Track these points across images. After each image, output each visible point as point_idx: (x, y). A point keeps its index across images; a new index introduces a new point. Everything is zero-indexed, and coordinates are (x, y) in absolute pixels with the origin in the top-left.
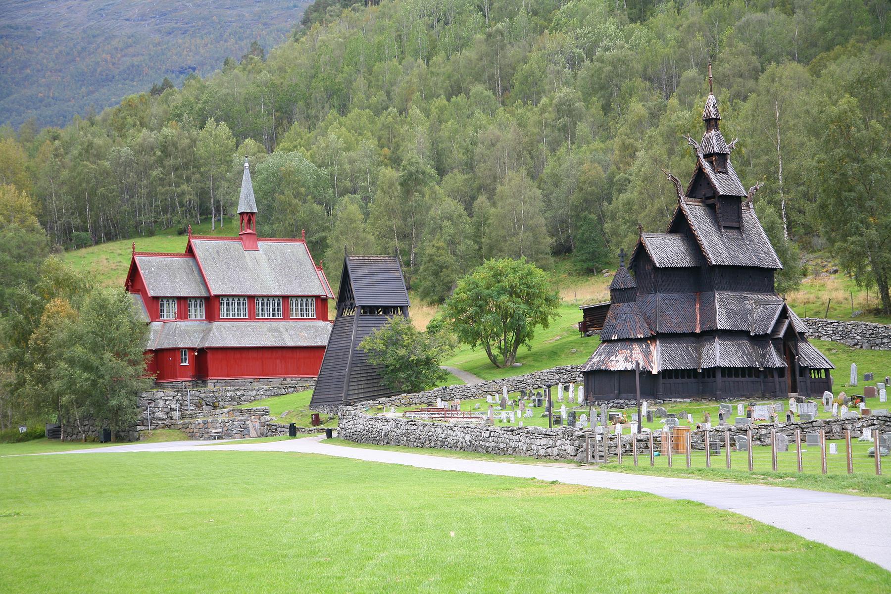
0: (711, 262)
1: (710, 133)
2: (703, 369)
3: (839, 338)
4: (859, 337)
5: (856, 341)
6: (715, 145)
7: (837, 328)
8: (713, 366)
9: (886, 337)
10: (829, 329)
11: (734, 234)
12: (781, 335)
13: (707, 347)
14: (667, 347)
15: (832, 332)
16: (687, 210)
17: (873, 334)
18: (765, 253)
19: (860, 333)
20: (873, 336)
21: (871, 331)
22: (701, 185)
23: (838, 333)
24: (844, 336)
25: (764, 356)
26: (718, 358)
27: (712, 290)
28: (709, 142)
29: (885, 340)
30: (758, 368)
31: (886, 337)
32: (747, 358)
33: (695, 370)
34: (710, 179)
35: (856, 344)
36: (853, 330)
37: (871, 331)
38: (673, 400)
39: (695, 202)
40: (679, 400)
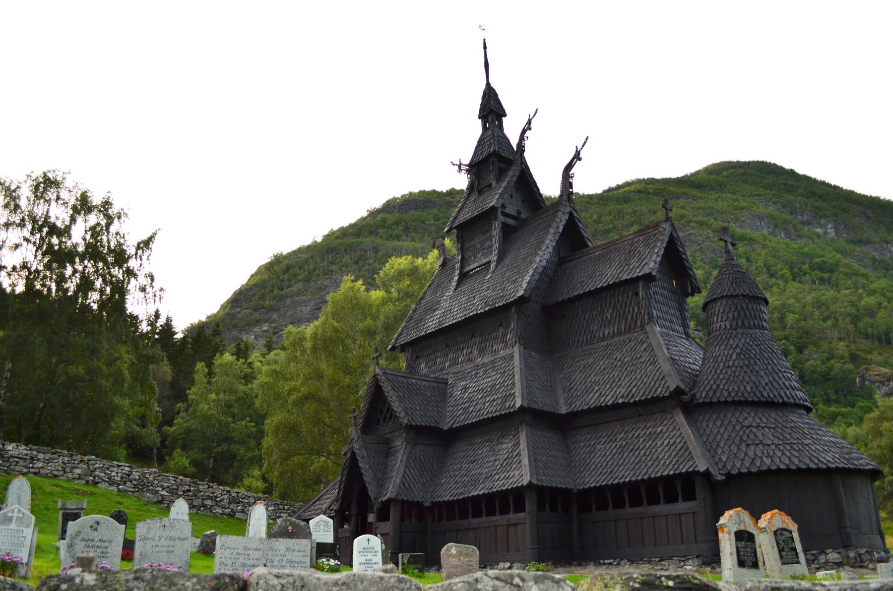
3: (131, 490)
4: (164, 493)
5: (160, 498)
7: (128, 475)
9: (210, 498)
10: (114, 474)
15: (119, 479)
17: (189, 491)
19: (168, 487)
20: (191, 494)
21: (188, 487)
23: (131, 481)
24: (141, 487)
29: (209, 502)
31: (210, 498)
35: (161, 502)
36: (156, 482)
37: (188, 487)
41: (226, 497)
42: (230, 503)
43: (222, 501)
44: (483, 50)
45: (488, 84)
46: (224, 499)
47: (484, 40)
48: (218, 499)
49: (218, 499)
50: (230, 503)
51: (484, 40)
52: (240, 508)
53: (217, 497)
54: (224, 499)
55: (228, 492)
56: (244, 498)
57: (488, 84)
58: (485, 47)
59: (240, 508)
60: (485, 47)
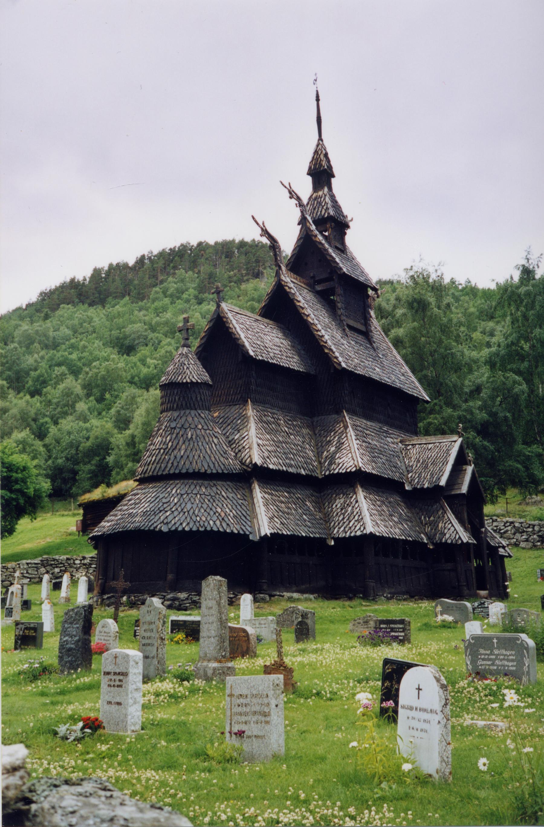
0: (339, 364)
1: (320, 193)
2: (337, 540)
6: (329, 206)
8: (359, 533)
11: (360, 338)
12: (464, 489)
13: (339, 502)
14: (272, 494)
16: (292, 285)
18: (403, 375)
22: (306, 264)
25: (434, 524)
26: (368, 519)
27: (338, 412)
28: (320, 203)
30: (426, 544)
32: (408, 525)
33: (321, 541)
34: (326, 250)
38: (287, 594)
39: (300, 282)
40: (296, 595)
41: (509, 528)
42: (514, 534)
43: (506, 532)
44: (316, 102)
45: (320, 139)
46: (507, 531)
47: (317, 91)
48: (502, 531)
49: (502, 531)
50: (514, 534)
51: (317, 91)
52: (524, 537)
53: (500, 530)
54: (507, 531)
55: (512, 523)
56: (529, 527)
57: (320, 139)
58: (318, 100)
59: (524, 537)
60: (318, 100)
